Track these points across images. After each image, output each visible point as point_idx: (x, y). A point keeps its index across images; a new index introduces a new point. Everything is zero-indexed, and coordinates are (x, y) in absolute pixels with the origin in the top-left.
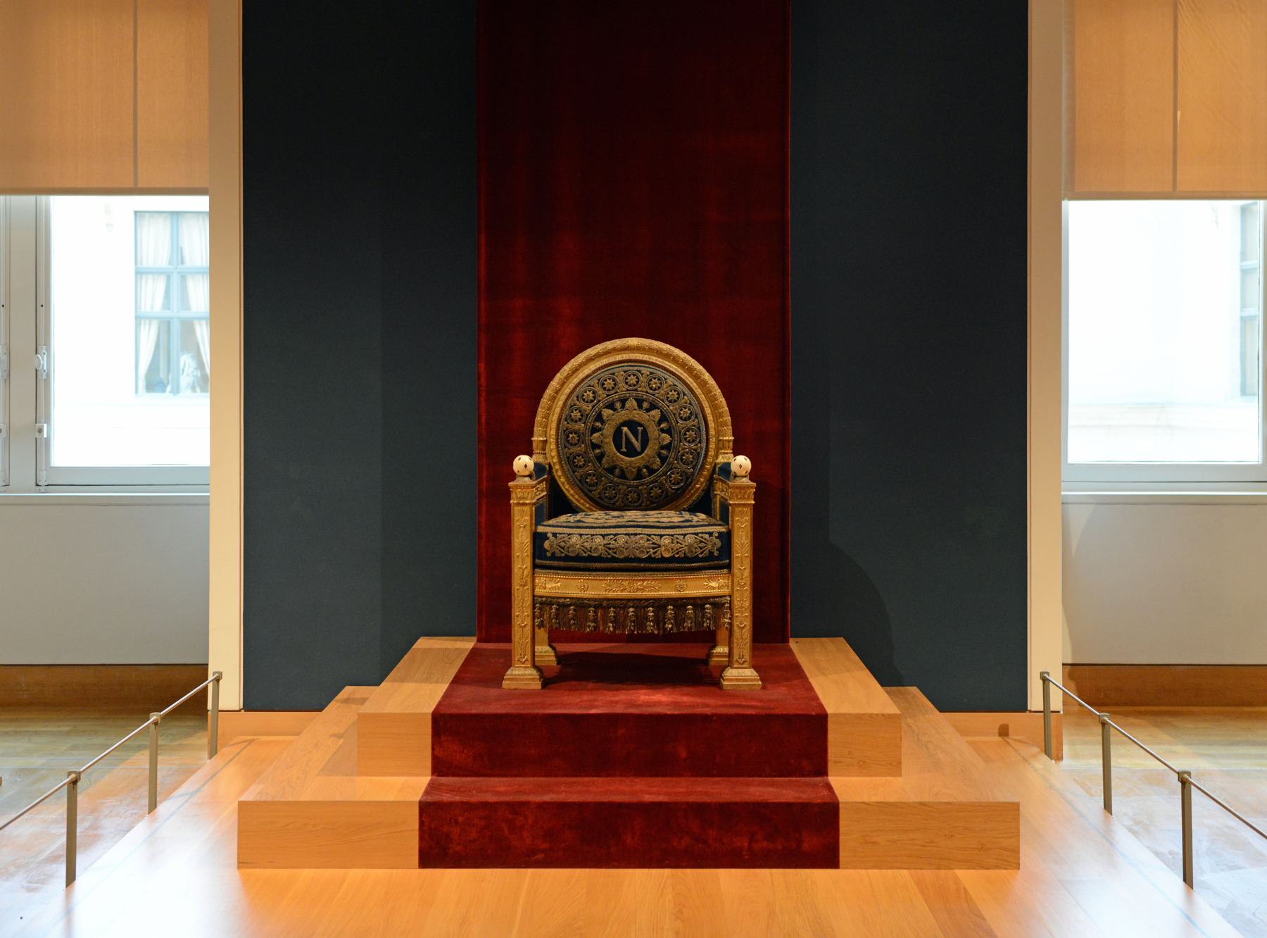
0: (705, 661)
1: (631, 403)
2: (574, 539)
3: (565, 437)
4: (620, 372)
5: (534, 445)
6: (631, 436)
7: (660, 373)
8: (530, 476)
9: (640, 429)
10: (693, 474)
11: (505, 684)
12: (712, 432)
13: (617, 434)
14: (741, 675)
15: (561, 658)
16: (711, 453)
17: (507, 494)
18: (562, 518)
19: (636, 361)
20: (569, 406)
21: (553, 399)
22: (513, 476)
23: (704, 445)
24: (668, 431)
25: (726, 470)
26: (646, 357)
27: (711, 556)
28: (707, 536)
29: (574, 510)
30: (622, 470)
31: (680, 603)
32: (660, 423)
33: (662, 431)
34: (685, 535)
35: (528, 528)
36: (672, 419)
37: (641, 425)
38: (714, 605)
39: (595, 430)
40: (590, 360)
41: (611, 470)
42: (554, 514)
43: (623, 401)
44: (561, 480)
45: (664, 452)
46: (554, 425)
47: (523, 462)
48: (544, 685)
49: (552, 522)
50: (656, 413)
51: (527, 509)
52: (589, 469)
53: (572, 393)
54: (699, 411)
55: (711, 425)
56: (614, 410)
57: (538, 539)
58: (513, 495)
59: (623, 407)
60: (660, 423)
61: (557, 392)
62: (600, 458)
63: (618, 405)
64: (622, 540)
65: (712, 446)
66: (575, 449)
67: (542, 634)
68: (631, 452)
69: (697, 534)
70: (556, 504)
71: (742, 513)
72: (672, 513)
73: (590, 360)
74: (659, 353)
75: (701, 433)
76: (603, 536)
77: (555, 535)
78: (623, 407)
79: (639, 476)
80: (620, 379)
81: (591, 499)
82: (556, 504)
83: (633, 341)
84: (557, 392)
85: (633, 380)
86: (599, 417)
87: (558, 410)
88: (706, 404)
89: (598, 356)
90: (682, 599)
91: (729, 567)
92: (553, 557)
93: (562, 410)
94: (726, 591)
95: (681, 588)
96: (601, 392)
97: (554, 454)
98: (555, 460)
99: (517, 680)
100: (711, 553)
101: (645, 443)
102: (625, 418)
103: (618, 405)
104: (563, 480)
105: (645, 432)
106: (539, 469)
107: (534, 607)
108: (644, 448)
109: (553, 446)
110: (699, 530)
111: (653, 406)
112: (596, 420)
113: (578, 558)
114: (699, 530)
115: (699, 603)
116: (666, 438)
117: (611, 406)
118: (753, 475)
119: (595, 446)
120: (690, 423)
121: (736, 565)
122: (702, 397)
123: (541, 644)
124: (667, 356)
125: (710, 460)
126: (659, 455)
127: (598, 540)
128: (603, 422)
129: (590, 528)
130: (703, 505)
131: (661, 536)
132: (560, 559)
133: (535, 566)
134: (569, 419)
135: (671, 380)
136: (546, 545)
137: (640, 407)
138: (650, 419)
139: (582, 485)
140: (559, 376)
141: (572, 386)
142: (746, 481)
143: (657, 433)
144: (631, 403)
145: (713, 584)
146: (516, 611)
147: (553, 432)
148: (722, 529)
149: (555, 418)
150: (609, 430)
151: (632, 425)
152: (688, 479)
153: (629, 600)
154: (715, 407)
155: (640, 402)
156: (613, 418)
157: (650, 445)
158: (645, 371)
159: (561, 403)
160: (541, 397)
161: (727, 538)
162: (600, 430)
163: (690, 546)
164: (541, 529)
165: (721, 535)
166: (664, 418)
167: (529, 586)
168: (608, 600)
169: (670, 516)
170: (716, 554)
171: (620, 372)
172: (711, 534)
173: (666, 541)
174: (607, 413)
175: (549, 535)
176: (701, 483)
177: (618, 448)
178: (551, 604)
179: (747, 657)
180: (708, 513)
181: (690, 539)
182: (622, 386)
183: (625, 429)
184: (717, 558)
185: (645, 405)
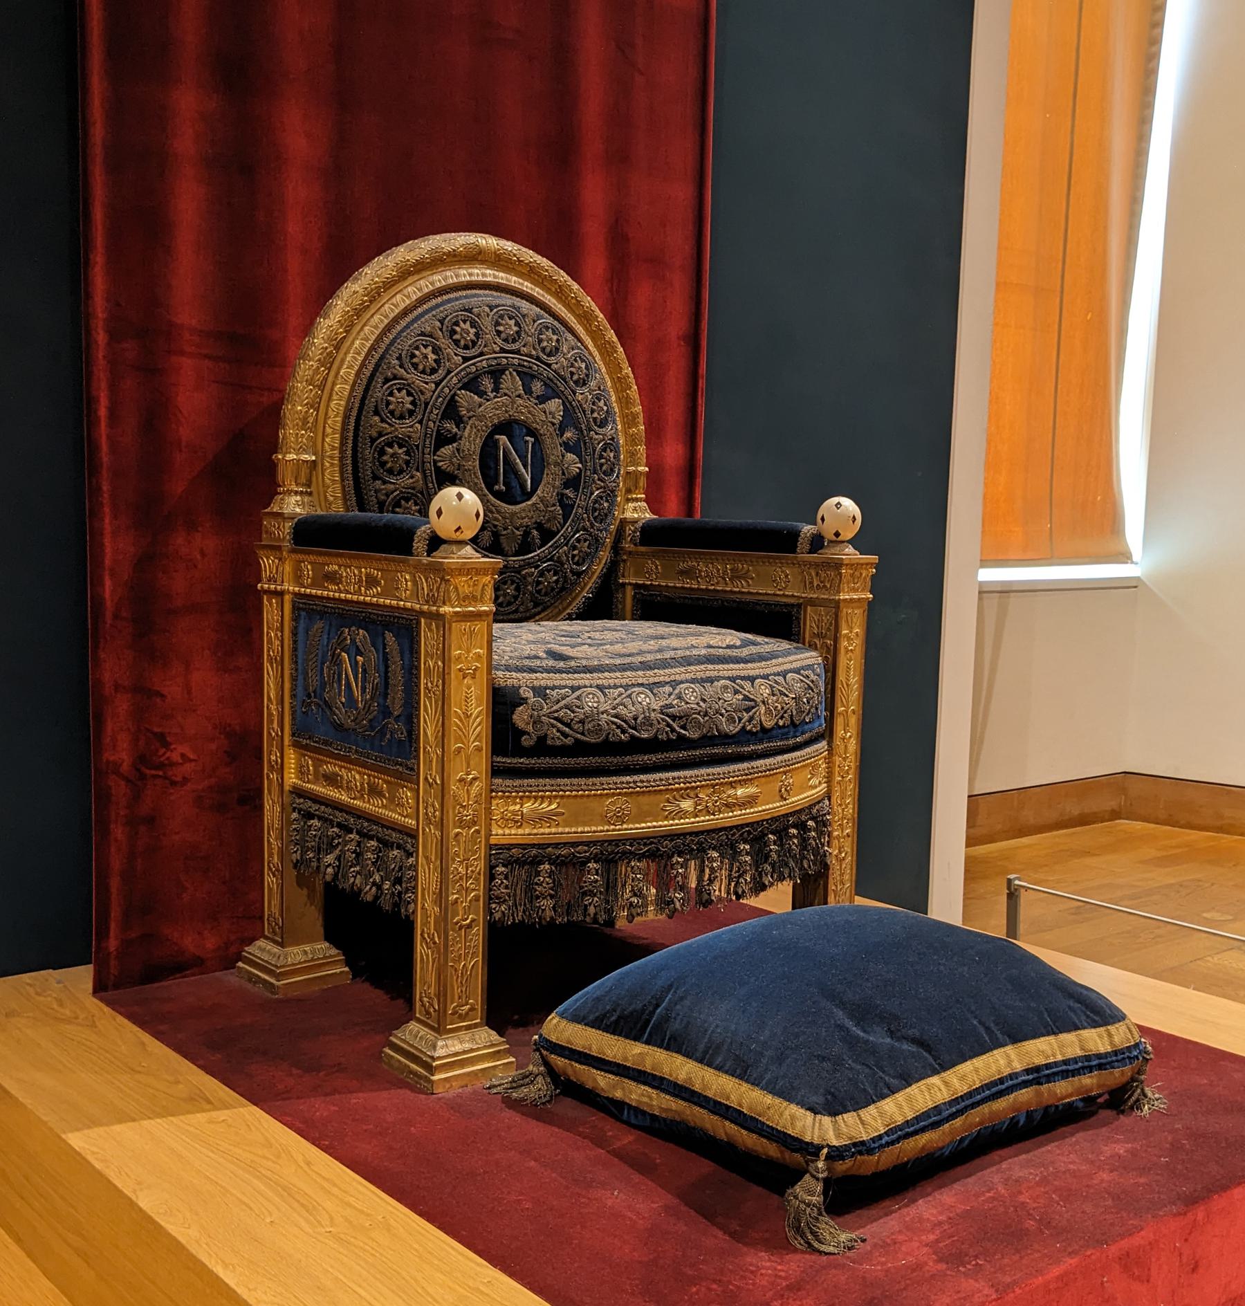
13: (489, 447)
21: (328, 362)
32: (562, 429)
37: (532, 432)
39: (443, 440)
43: (496, 373)
50: (554, 405)
59: (496, 389)
63: (487, 383)
76: (652, 687)
77: (540, 691)
78: (496, 389)
80: (487, 323)
86: (451, 411)
92: (542, 747)
103: (487, 383)
117: (472, 384)
128: (459, 421)
131: (752, 679)
133: (496, 772)
136: (520, 717)
174: (466, 399)
175: (526, 693)
178: (536, 862)
183: (503, 439)
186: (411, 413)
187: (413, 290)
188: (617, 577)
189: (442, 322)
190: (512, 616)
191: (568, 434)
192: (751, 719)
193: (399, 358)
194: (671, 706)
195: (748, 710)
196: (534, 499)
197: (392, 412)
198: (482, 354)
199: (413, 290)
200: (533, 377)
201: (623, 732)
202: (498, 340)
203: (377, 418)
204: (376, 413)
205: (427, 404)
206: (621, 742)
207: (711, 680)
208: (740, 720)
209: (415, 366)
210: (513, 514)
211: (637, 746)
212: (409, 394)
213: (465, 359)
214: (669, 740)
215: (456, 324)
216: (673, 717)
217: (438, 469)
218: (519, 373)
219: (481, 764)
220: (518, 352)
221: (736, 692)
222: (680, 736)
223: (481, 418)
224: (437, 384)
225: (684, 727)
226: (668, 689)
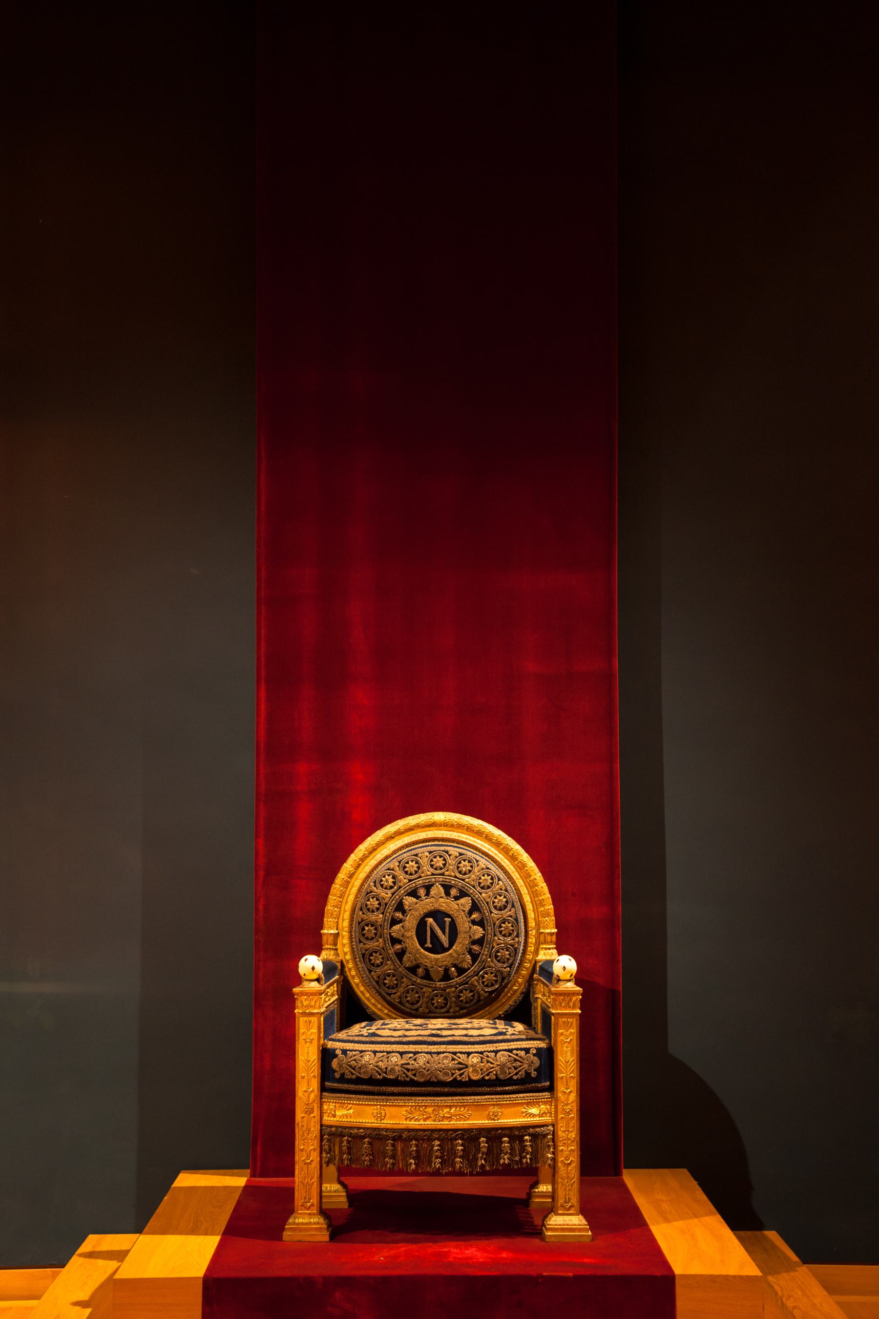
0: (526, 1202)
1: (437, 890)
2: (367, 1058)
3: (361, 929)
4: (424, 852)
5: (324, 938)
6: (436, 930)
7: (470, 854)
8: (318, 980)
9: (448, 920)
10: (509, 974)
11: (287, 1235)
12: (532, 923)
13: (421, 926)
14: (567, 1223)
15: (352, 1196)
16: (531, 948)
17: (291, 1001)
18: (356, 1029)
19: (443, 840)
20: (365, 893)
22: (298, 980)
23: (522, 939)
24: (481, 923)
25: (546, 971)
26: (454, 835)
28: (522, 1053)
29: (370, 1018)
30: (427, 971)
31: (494, 1134)
32: (470, 913)
33: (474, 922)
34: (496, 1052)
35: (315, 1042)
36: (484, 907)
37: (449, 916)
38: (535, 1137)
39: (394, 922)
40: (390, 838)
41: (413, 970)
42: (346, 1022)
43: (428, 888)
44: (355, 981)
45: (476, 947)
46: (347, 915)
47: (310, 964)
48: (333, 1237)
49: (342, 1035)
50: (466, 902)
51: (314, 1019)
52: (389, 968)
53: (368, 877)
54: (515, 897)
55: (531, 915)
56: (418, 897)
57: (326, 1055)
58: (298, 1004)
59: (428, 894)
60: (470, 913)
61: (351, 876)
62: (400, 955)
63: (422, 892)
64: (422, 1060)
65: (532, 940)
66: (371, 945)
67: (332, 1170)
68: (437, 948)
69: (510, 1051)
70: (350, 1011)
71: (568, 1026)
72: (484, 1022)
73: (390, 838)
74: (469, 829)
75: (518, 924)
76: (402, 1054)
77: (344, 1052)
78: (428, 894)
79: (446, 977)
80: (424, 861)
81: (390, 1004)
82: (350, 1011)
83: (439, 816)
84: (351, 876)
85: (439, 862)
86: (400, 907)
87: (352, 898)
88: (524, 891)
89: (399, 833)
90: (496, 1129)
91: (551, 1089)
92: (343, 1079)
93: (356, 897)
94: (547, 1119)
95: (495, 1116)
96: (401, 876)
97: (347, 949)
98: (348, 957)
99: (300, 1230)
100: (528, 1074)
101: (452, 941)
102: (430, 908)
103: (422, 892)
104: (357, 980)
105: (453, 924)
106: (329, 969)
107: (322, 1140)
108: (452, 942)
109: (346, 941)
110: (513, 1045)
111: (463, 894)
112: (396, 910)
113: (371, 1081)
114: (513, 1045)
115: (516, 1134)
116: (478, 931)
117: (414, 893)
118: (579, 979)
119: (394, 941)
120: (506, 913)
121: (560, 1087)
122: (520, 883)
123: (330, 1182)
124: (479, 833)
125: (529, 957)
126: (470, 952)
127: (395, 1059)
128: (404, 912)
129: (388, 1040)
130: (521, 1012)
131: (469, 1054)
132: (350, 1081)
133: (323, 1089)
134: (365, 908)
135: (483, 862)
136: (335, 1064)
137: (448, 894)
138: (459, 908)
139: (379, 986)
140: (353, 858)
141: (368, 869)
142: (571, 986)
143: (467, 925)
144: (437, 890)
145: (534, 1110)
146: (299, 1145)
147: (346, 924)
148: (542, 1045)
149: (348, 907)
150: (411, 922)
151: (438, 915)
152: (504, 980)
153: (433, 1131)
154: (534, 894)
155: (447, 888)
156: (417, 907)
157: (459, 940)
158: (454, 851)
159: (355, 890)
160: (331, 881)
161: (548, 1056)
162: (401, 921)
163: (502, 1066)
164: (330, 1045)
165: (539, 1052)
166: (475, 907)
167: (316, 1113)
168: (409, 1130)
169: (482, 1027)
170: (534, 1074)
171: (424, 852)
172: (527, 1050)
174: (409, 901)
175: (338, 1052)
176: (518, 986)
177: (422, 943)
178: (342, 1135)
179: (575, 1200)
180: (527, 1021)
181: (502, 1057)
182: (427, 870)
183: (430, 920)
184: (537, 1080)
185: (454, 892)
186: (378, 909)
187: (392, 846)
188: (534, 993)
189: (400, 862)
190: (446, 1014)
191: (474, 916)
192: (461, 1075)
193: (375, 882)
194: (408, 1064)
195: (459, 1069)
196: (451, 951)
197: (368, 910)
198: (420, 877)
199: (392, 846)
200: (451, 887)
201: (380, 1074)
202: (432, 870)
203: (361, 913)
204: (361, 909)
205: (386, 904)
206: (378, 1080)
207: (438, 1053)
208: (453, 1074)
209: (382, 886)
210: (437, 960)
211: (386, 1082)
212: (378, 899)
213: (410, 881)
214: (405, 1081)
215: (408, 863)
216: (408, 1070)
217: (391, 937)
218: (442, 885)
219: (315, 1084)
220: (443, 874)
221: (453, 1059)
222: (412, 1080)
223: (416, 910)
224: (393, 894)
225: (414, 1075)
226: (411, 1055)
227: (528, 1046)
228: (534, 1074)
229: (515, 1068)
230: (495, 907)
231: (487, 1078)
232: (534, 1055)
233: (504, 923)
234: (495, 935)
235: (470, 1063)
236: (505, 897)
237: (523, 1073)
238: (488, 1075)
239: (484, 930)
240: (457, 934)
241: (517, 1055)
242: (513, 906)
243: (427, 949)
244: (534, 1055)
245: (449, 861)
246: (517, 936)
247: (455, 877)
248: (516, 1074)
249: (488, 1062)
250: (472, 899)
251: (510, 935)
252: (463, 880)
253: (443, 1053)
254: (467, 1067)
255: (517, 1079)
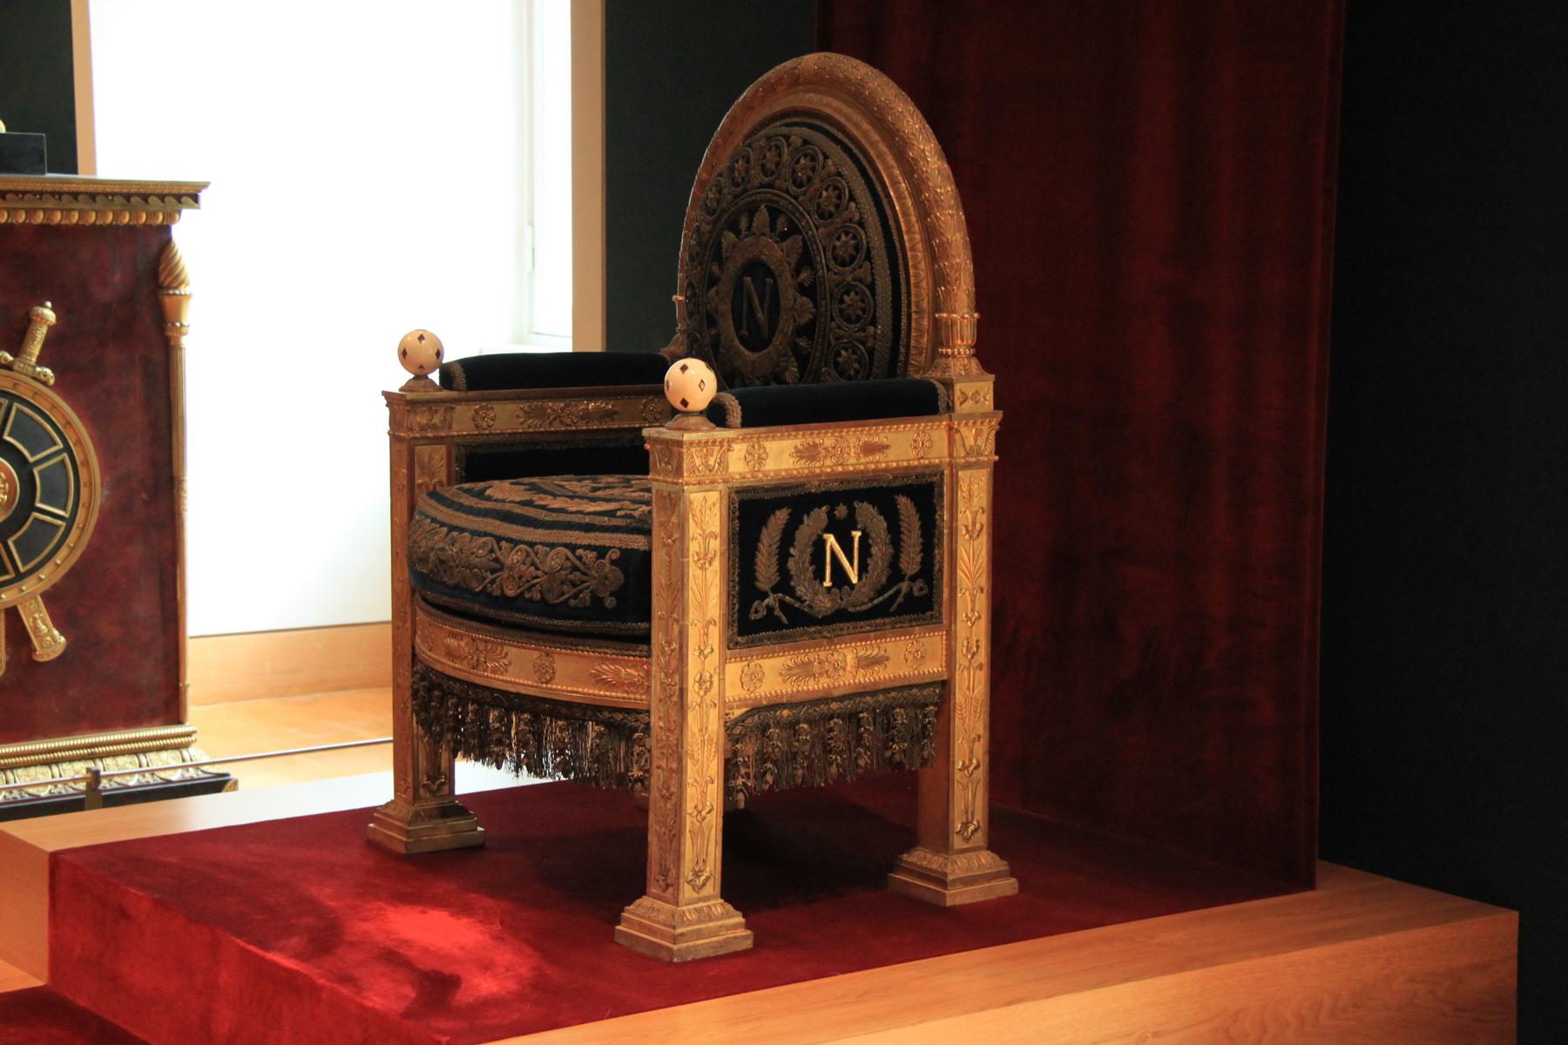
9: (769, 280)
27: (596, 609)
28: (590, 556)
32: (797, 271)
50: (795, 242)
69: (573, 548)
100: (597, 600)
131: (514, 542)
135: (838, 160)
155: (774, 213)
163: (551, 574)
170: (610, 602)
172: (602, 551)
173: (515, 557)
191: (803, 276)
195: (493, 571)
227: (602, 543)
228: (610, 602)
229: (575, 585)
230: (835, 258)
231: (527, 596)
232: (613, 562)
233: (848, 293)
234: (832, 319)
235: (508, 562)
236: (854, 237)
237: (586, 596)
238: (529, 589)
239: (816, 306)
240: (778, 313)
241: (580, 558)
242: (868, 257)
243: (743, 341)
244: (613, 562)
245: (785, 156)
246: (874, 323)
247: (787, 192)
248: (576, 596)
249: (533, 564)
250: (804, 240)
251: (858, 319)
252: (796, 198)
253: (486, 534)
254: (502, 565)
255: (576, 608)
